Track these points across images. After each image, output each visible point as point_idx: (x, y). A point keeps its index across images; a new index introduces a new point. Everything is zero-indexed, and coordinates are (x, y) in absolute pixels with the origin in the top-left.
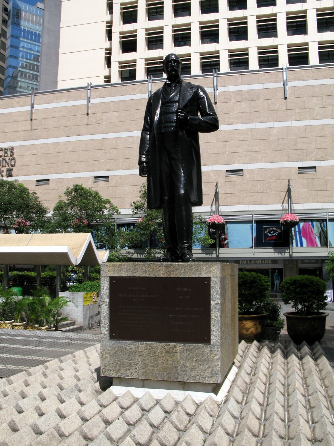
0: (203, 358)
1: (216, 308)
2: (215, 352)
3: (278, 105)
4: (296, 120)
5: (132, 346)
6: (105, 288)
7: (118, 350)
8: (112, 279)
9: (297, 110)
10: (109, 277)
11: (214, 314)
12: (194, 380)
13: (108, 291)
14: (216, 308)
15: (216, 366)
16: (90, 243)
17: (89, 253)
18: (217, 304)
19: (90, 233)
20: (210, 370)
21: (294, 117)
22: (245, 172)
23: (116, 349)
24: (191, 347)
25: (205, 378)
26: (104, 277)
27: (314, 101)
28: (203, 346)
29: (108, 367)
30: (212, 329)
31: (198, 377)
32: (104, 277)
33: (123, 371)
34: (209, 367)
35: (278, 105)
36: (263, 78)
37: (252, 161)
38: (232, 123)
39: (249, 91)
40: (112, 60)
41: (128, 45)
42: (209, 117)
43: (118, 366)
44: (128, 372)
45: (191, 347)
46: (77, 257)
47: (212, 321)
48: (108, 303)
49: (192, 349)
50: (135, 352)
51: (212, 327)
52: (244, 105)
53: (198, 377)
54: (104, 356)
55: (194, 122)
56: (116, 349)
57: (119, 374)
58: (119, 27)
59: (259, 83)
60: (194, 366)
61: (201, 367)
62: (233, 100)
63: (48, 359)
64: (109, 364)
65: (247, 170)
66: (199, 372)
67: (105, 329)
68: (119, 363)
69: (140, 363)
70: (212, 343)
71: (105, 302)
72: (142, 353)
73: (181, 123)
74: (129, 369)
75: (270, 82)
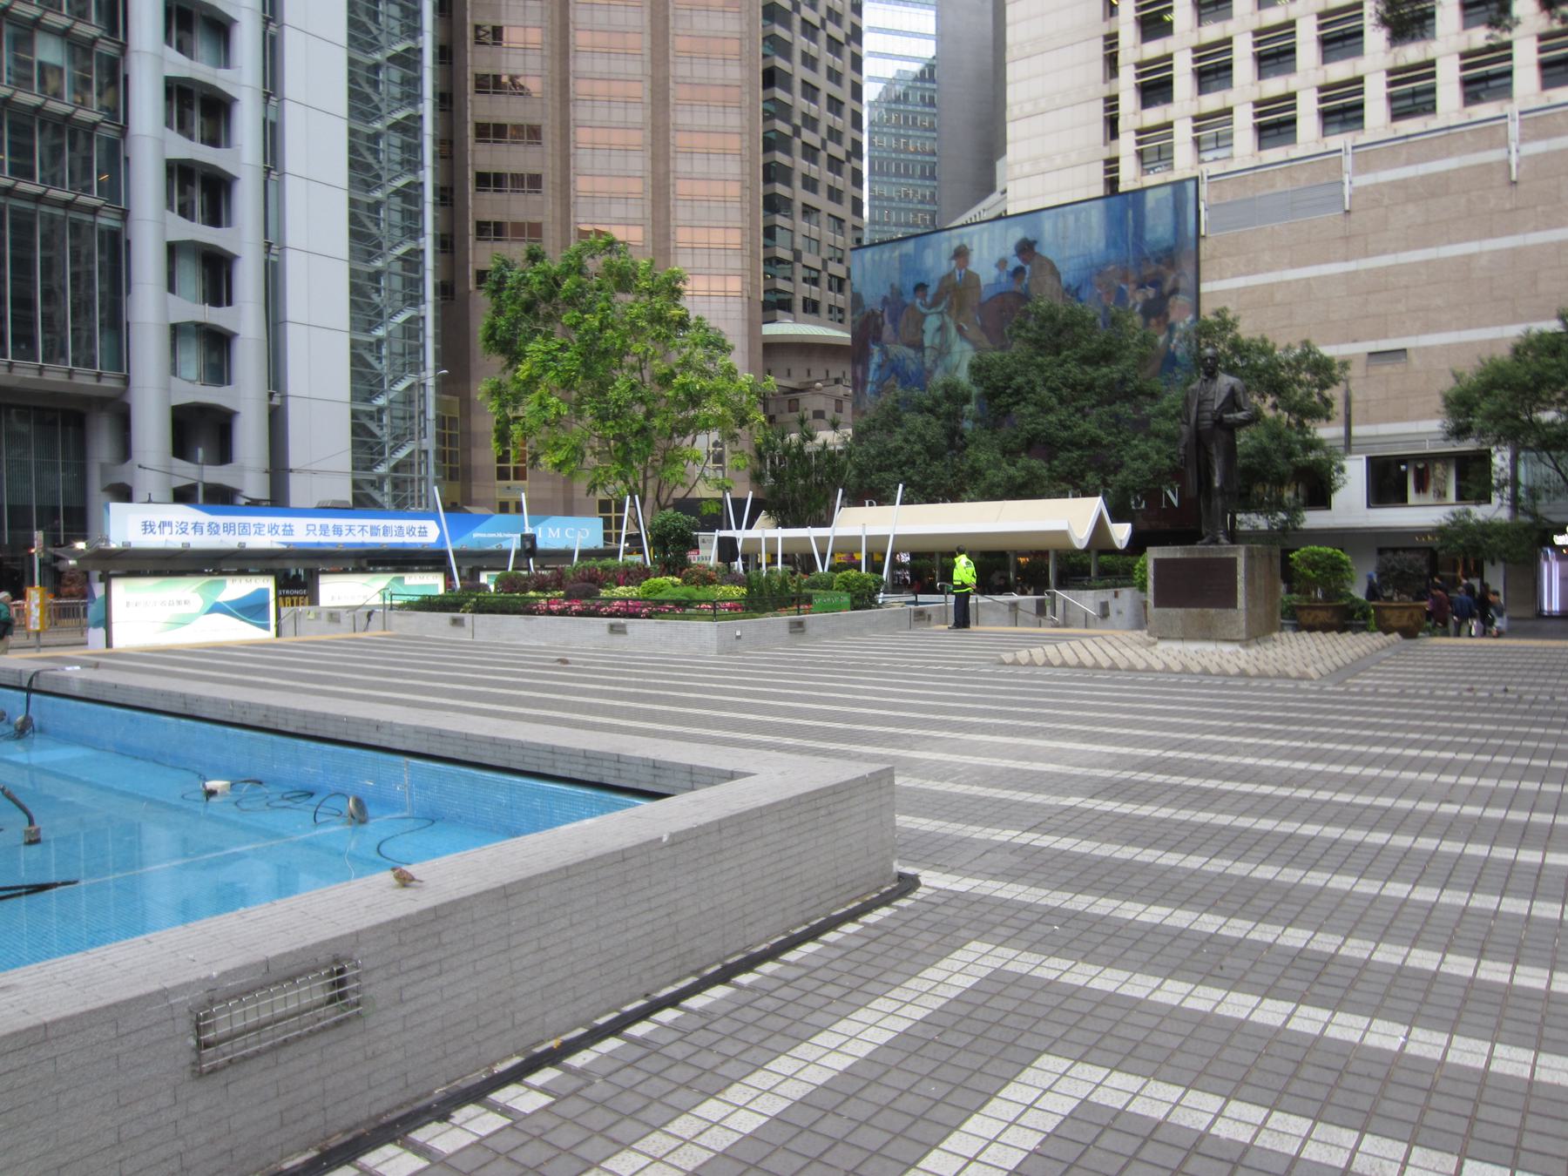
4: (1536, 229)
9: (1540, 209)
16: (1101, 517)
17: (1100, 529)
19: (1100, 499)
22: (1411, 354)
37: (1428, 328)
38: (1384, 252)
40: (1122, 125)
41: (1156, 89)
46: (1081, 536)
52: (1411, 209)
58: (1132, 49)
59: (1449, 155)
62: (1386, 201)
65: (1417, 349)
73: (1219, 423)
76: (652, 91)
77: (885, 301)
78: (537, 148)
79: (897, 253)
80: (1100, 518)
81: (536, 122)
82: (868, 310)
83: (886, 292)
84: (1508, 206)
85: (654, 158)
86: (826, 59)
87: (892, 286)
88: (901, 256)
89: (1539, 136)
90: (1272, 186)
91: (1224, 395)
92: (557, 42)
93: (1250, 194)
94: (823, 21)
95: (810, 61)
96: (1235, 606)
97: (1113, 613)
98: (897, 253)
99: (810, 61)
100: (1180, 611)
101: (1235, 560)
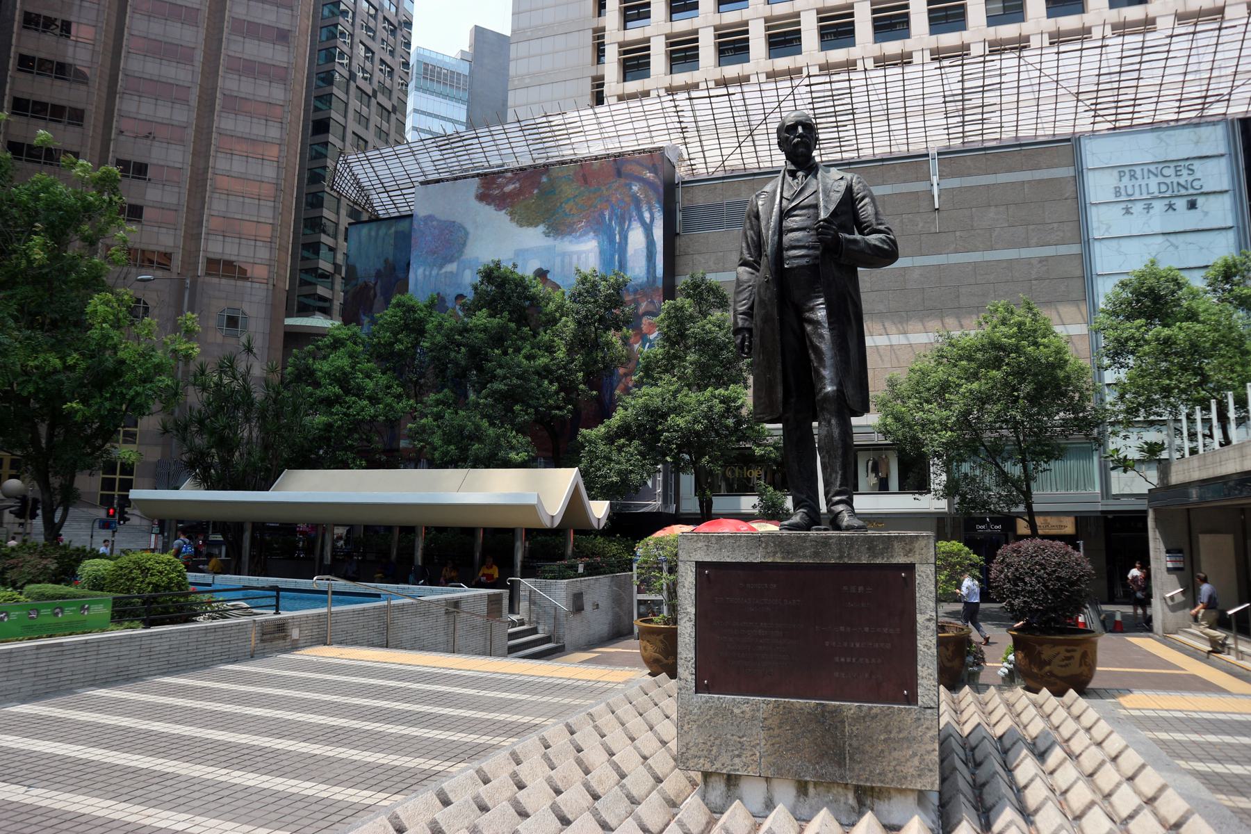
0: (901, 736)
1: (927, 628)
2: (927, 723)
3: (921, 225)
5: (745, 707)
6: (686, 584)
7: (716, 714)
8: (700, 565)
9: (958, 234)
10: (697, 562)
11: (924, 642)
12: (882, 782)
13: (693, 592)
14: (927, 628)
15: (928, 752)
17: (575, 506)
18: (929, 620)
20: (916, 761)
21: (952, 247)
23: (712, 712)
24: (874, 711)
25: (905, 778)
26: (685, 562)
27: (991, 215)
28: (900, 710)
29: (693, 751)
30: (920, 673)
31: (890, 775)
32: (685, 562)
33: (725, 758)
34: (915, 754)
35: (921, 225)
36: (892, 173)
39: (1037, 167)
42: (881, 236)
43: (715, 749)
44: (737, 760)
45: (874, 711)
47: (919, 657)
48: (693, 617)
49: (877, 715)
50: (753, 718)
51: (919, 668)
53: (890, 775)
54: (686, 728)
55: (852, 247)
56: (712, 712)
57: (718, 765)
60: (882, 751)
61: (896, 754)
63: (537, 721)
64: (696, 745)
66: (894, 763)
67: (686, 669)
68: (717, 742)
69: (763, 742)
70: (920, 703)
71: (687, 613)
72: (767, 723)
74: (739, 756)
75: (905, 182)
76: (200, 97)
77: (379, 274)
78: (78, 129)
79: (393, 230)
80: (576, 491)
81: (80, 106)
82: (360, 282)
83: (380, 265)
84: (933, 230)
85: (195, 154)
86: (375, 119)
87: (386, 261)
88: (396, 232)
89: (953, 175)
90: (738, 195)
91: (836, 197)
92: (111, 43)
93: (718, 201)
94: (375, 92)
95: (363, 120)
96: (912, 699)
97: (588, 607)
98: (393, 230)
99: (363, 120)
100: (761, 704)
101: (910, 568)
